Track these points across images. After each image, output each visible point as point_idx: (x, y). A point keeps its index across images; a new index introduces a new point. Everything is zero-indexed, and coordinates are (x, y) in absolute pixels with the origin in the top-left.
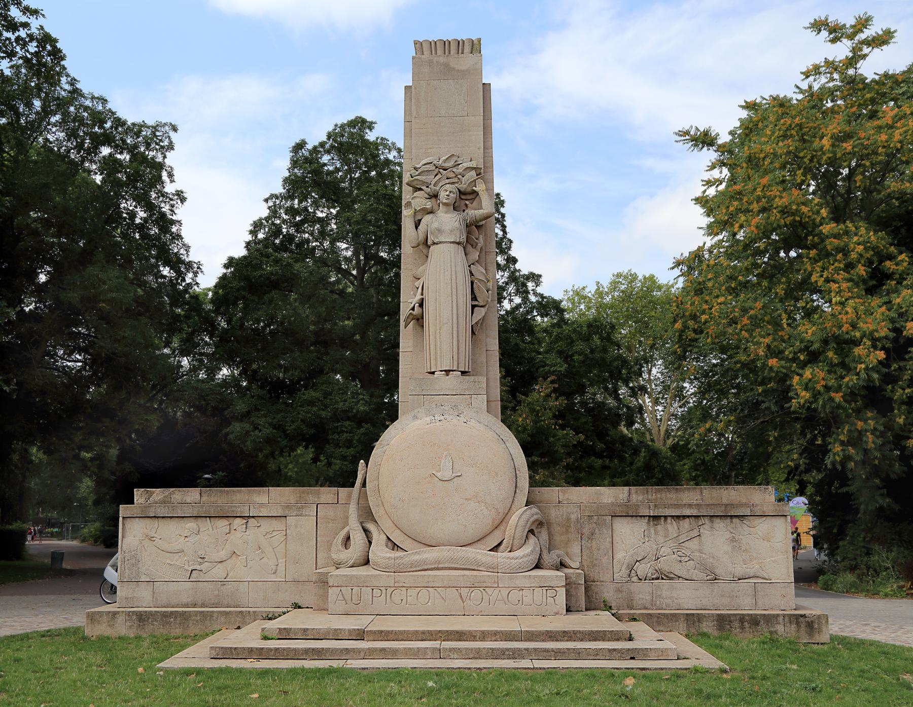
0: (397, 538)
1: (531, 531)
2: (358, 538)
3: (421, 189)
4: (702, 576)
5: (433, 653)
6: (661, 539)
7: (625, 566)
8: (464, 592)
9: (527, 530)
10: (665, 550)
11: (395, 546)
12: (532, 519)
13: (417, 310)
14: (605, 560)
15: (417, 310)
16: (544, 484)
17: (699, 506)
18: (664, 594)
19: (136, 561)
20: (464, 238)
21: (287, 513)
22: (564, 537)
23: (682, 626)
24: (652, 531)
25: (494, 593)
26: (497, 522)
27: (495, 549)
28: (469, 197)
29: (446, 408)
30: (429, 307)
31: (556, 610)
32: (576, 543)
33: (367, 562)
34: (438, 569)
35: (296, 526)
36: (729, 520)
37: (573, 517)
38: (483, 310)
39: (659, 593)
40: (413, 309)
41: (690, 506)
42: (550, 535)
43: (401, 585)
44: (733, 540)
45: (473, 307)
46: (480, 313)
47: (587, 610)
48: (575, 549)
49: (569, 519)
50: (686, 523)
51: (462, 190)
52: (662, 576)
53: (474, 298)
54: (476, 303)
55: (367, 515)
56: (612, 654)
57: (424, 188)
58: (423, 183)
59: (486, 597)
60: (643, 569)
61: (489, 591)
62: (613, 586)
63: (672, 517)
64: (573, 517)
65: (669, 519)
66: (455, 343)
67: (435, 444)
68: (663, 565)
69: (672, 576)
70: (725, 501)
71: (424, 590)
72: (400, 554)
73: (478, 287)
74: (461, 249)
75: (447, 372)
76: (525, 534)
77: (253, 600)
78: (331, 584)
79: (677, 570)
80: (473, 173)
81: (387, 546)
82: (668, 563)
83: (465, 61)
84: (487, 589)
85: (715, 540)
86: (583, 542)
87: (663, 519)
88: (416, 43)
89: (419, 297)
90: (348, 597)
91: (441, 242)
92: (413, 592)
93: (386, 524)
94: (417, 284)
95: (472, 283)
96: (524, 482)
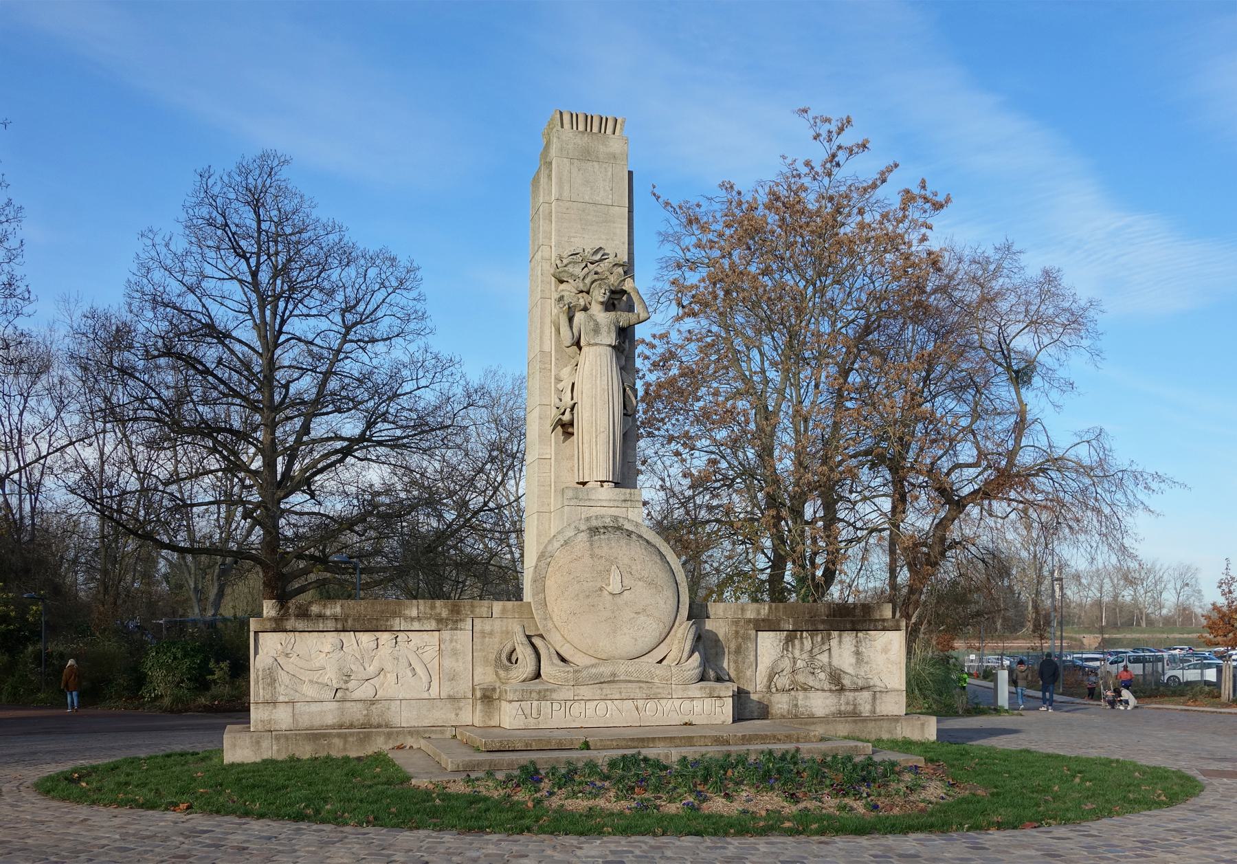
6: (797, 653)
8: (640, 703)
13: (567, 417)
14: (749, 673)
25: (667, 705)
35: (451, 641)
40: (563, 414)
44: (858, 653)
61: (663, 702)
68: (801, 678)
71: (602, 703)
90: (527, 711)
92: (591, 705)
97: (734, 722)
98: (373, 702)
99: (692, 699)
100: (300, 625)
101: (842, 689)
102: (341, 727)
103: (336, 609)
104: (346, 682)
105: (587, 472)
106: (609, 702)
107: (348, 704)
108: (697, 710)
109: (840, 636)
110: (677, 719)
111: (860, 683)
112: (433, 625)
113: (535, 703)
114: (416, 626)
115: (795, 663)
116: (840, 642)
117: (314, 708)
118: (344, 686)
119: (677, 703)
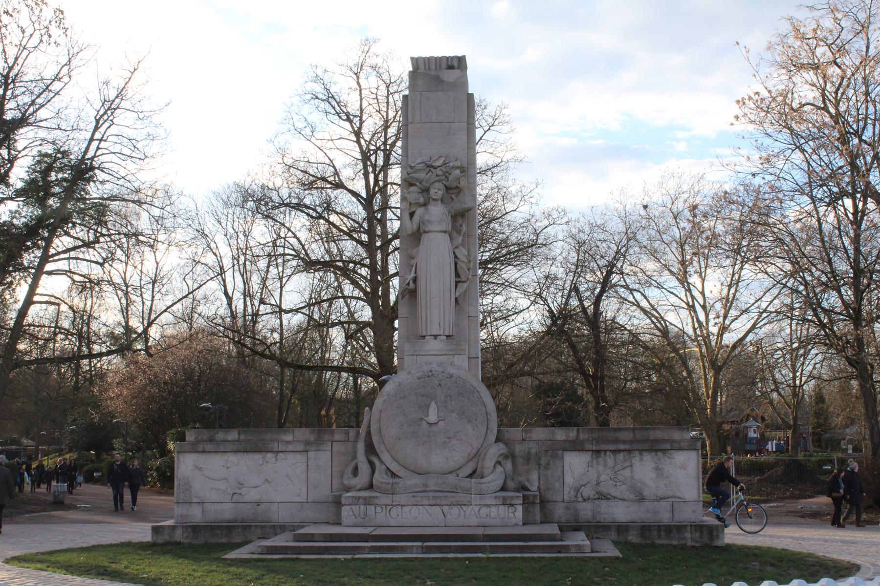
0: (394, 467)
1: (499, 463)
2: (364, 467)
3: (415, 185)
4: (632, 496)
6: (601, 468)
8: (446, 508)
9: (494, 462)
11: (394, 475)
12: (499, 453)
13: (412, 286)
14: (557, 485)
15: (412, 286)
16: (506, 426)
17: (631, 442)
18: (603, 510)
19: (188, 487)
20: (450, 228)
21: (308, 448)
22: (525, 467)
23: (614, 535)
24: (595, 462)
25: (468, 510)
27: (471, 476)
28: (454, 191)
30: (421, 284)
33: (371, 487)
35: (315, 459)
36: (654, 454)
37: (533, 451)
38: (465, 285)
40: (408, 284)
41: (624, 442)
42: (514, 465)
44: (657, 469)
45: (457, 283)
46: (463, 287)
47: (541, 523)
48: (534, 476)
49: (529, 453)
50: (621, 456)
52: (602, 496)
53: (457, 275)
56: (544, 549)
57: (418, 184)
58: (417, 180)
59: (462, 513)
60: (587, 492)
62: (564, 504)
64: (533, 451)
65: (608, 453)
68: (603, 489)
70: (652, 438)
71: (415, 508)
72: (397, 480)
73: (462, 267)
74: (447, 236)
75: (436, 337)
77: (282, 515)
78: (343, 503)
79: (614, 492)
80: (458, 172)
81: (387, 474)
83: (450, 76)
85: (644, 469)
89: (412, 275)
91: (430, 231)
93: (386, 457)
94: (412, 262)
95: (456, 264)
96: (494, 426)
97: (524, 524)
98: (258, 504)
99: (488, 506)
100: (208, 447)
101: (641, 499)
102: (235, 521)
103: (233, 435)
104: (240, 489)
105: (424, 329)
107: (241, 505)
108: (492, 515)
109: (641, 455)
110: (474, 521)
111: (661, 493)
113: (362, 507)
114: (290, 448)
116: (641, 459)
117: (218, 507)
118: (238, 491)
119: (476, 508)
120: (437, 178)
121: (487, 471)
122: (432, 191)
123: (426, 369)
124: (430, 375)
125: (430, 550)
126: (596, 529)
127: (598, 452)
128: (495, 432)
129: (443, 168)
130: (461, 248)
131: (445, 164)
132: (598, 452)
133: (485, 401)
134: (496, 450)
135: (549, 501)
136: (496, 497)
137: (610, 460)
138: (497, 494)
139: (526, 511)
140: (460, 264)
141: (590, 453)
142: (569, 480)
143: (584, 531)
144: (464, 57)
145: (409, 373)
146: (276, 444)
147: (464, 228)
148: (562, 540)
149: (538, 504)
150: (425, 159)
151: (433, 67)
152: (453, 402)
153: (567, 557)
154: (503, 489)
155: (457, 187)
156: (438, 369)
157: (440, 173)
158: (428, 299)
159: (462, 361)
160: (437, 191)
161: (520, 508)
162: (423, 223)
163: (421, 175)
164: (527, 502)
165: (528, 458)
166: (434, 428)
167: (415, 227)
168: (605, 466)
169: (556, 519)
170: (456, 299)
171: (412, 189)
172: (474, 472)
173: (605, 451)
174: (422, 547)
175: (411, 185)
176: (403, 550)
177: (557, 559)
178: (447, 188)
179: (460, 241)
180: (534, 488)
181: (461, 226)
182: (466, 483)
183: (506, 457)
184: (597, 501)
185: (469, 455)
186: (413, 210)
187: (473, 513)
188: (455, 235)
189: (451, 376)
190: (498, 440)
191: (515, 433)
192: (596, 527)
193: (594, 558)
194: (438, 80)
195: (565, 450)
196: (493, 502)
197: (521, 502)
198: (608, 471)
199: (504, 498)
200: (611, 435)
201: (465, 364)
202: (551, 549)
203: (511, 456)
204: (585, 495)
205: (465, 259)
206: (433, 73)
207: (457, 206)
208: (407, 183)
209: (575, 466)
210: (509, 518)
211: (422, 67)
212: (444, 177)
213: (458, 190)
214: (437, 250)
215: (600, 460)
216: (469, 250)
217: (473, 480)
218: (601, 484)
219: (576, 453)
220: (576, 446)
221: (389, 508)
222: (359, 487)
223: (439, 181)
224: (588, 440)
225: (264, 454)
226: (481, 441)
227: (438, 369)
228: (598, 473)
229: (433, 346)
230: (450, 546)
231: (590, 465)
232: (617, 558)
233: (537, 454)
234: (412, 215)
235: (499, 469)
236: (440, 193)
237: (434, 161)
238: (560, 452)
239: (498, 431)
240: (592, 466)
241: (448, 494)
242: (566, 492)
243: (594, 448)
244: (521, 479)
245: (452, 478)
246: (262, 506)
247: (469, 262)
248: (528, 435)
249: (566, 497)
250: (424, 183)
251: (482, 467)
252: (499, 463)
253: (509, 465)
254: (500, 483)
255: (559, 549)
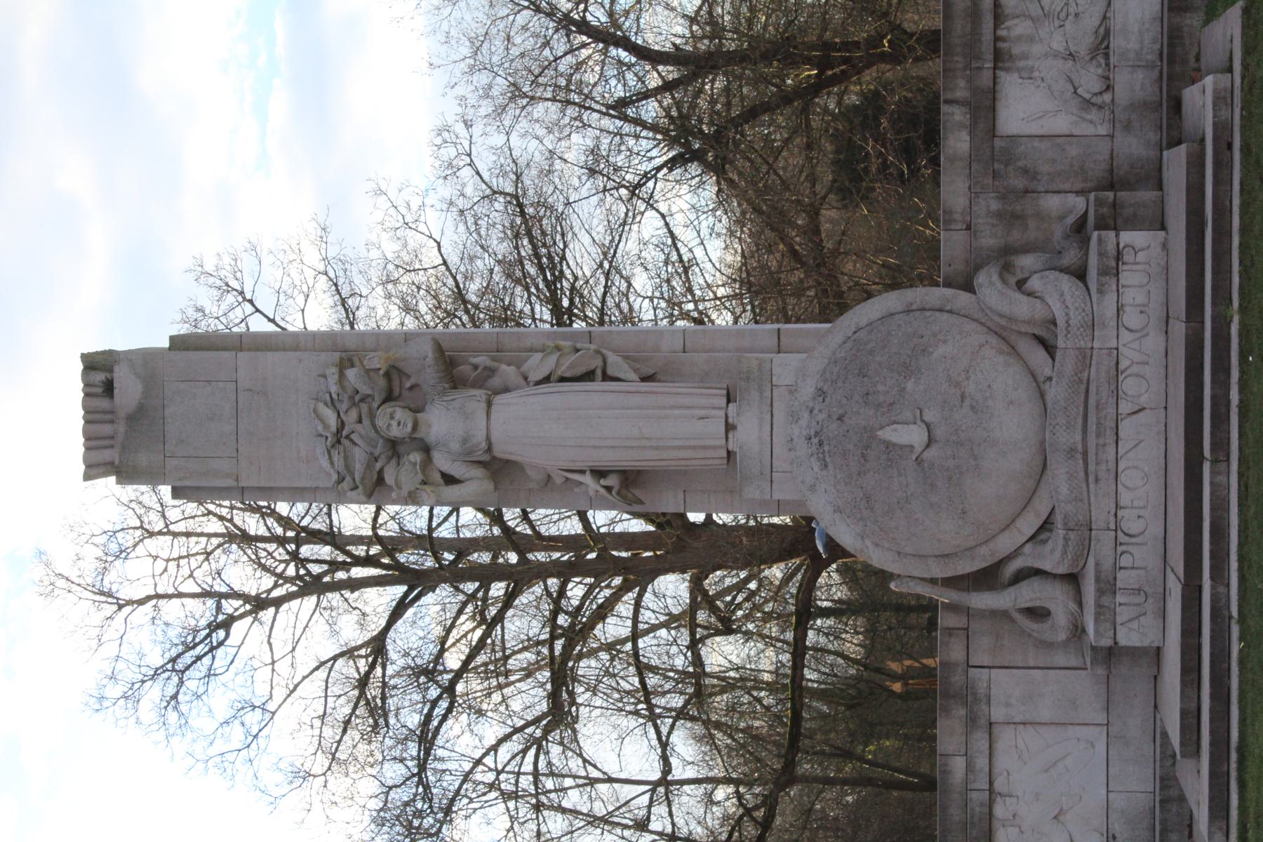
0: (1029, 524)
1: (1020, 284)
2: (1028, 594)
3: (381, 472)
5: (1219, 473)
6: (1036, 49)
7: (1084, 115)
8: (1125, 408)
10: (1057, 44)
11: (1046, 525)
12: (999, 285)
14: (1073, 151)
15: (612, 481)
18: (1133, 45)
20: (480, 393)
21: (983, 722)
22: (1032, 224)
23: (1193, 20)
24: (1022, 64)
26: (1005, 348)
27: (1050, 349)
28: (396, 383)
29: (797, 431)
30: (606, 459)
31: (1159, 249)
32: (1042, 202)
33: (1073, 579)
34: (1085, 454)
37: (995, 205)
38: (612, 358)
39: (1132, 55)
42: (1026, 249)
43: (1112, 519)
45: (606, 377)
46: (616, 364)
47: (1161, 189)
48: (1052, 203)
49: (999, 215)
51: (383, 396)
52: (1102, 47)
53: (588, 376)
54: (599, 372)
55: (987, 578)
56: (1222, 180)
57: (378, 466)
58: (369, 466)
59: (1135, 369)
60: (1090, 81)
61: (1124, 364)
63: (996, 27)
64: (995, 205)
66: (677, 412)
67: (863, 456)
68: (1083, 47)
69: (1102, 30)
71: (1122, 477)
72: (1058, 518)
73: (571, 367)
74: (498, 400)
75: (729, 427)
76: (1025, 299)
77: (1137, 784)
78: (1109, 642)
79: (1091, 20)
81: (1044, 542)
82: (1082, 34)
83: (129, 390)
84: (1121, 367)
86: (1041, 188)
87: (1001, 45)
88: (87, 477)
89: (587, 479)
91: (488, 438)
92: (1125, 498)
93: (1005, 544)
94: (559, 481)
95: (563, 379)
96: (936, 295)
97: (1163, 228)
105: (709, 454)
106: (1122, 466)
108: (1140, 299)
110: (1154, 342)
112: (980, 742)
113: (1120, 598)
115: (1056, 55)
119: (1126, 336)
120: (366, 421)
121: (1039, 311)
122: (395, 432)
123: (803, 449)
124: (817, 439)
125: (1220, 445)
126: (1177, 62)
127: (998, 56)
128: (949, 292)
129: (343, 407)
130: (525, 368)
131: (333, 404)
132: (998, 56)
133: (878, 315)
134: (992, 291)
135: (1111, 171)
136: (1100, 292)
137: (1017, 28)
138: (1093, 287)
139: (1133, 223)
140: (563, 370)
141: (1000, 73)
142: (1061, 124)
143: (1180, 89)
144: (85, 357)
145: (812, 488)
146: (974, 795)
147: (481, 360)
148: (1203, 140)
149: (1118, 195)
150: (320, 449)
151: (107, 429)
152: (880, 388)
153: (1242, 127)
154: (1080, 275)
155: (387, 375)
156: (803, 423)
157: (353, 414)
158: (648, 443)
159: (785, 368)
160: (396, 422)
161: (1126, 237)
162: (470, 453)
163: (359, 456)
164: (1113, 220)
165: (1011, 218)
166: (939, 432)
167: (478, 472)
168: (1031, 39)
169: (1153, 153)
170: (645, 379)
171: (389, 478)
172: (1042, 341)
173: (997, 39)
174: (1215, 462)
175: (380, 480)
176: (1220, 506)
177: (1246, 149)
178: (389, 398)
179: (511, 370)
180: (1079, 203)
181: (476, 367)
182: (1067, 361)
183: (1007, 268)
184: (1113, 60)
185: (1001, 352)
186: (438, 478)
187: (1136, 345)
188: (496, 382)
189: (821, 393)
190: (969, 287)
191: (953, 245)
192: (1171, 61)
193: (1245, 66)
194: (138, 417)
195: (992, 132)
196: (1111, 299)
197: (1112, 234)
198: (1043, 33)
199: (1103, 272)
200: (960, 26)
201: (793, 359)
202: (1222, 166)
203: (1005, 257)
204: (1097, 86)
205: (553, 359)
206: (122, 428)
207: (429, 376)
208: (375, 489)
209: (1031, 108)
210: (1148, 262)
211: (107, 455)
212: (364, 407)
213: (393, 373)
214: (528, 422)
215: (1016, 50)
216: (532, 350)
217: (1061, 343)
218: (1073, 48)
219: (999, 105)
220: (985, 107)
221: (1122, 538)
222: (1073, 606)
223: (372, 416)
224: (970, 80)
225: (996, 824)
226: (972, 326)
227: (803, 423)
228: (1046, 55)
229: (749, 434)
230: (1213, 397)
231: (1028, 75)
232: (1246, 11)
233: (1002, 198)
234: (449, 480)
235: (1035, 283)
236: (400, 414)
237: (326, 427)
238: (998, 143)
239: (948, 285)
240: (1032, 70)
241: (1092, 401)
242: (1091, 130)
243: (989, 65)
244: (1058, 232)
245: (1055, 392)
246: (1117, 828)
247: (558, 348)
248: (957, 217)
249: (1102, 130)
250: (377, 453)
251: (1030, 322)
252: (1020, 284)
253: (1026, 262)
254: (1067, 284)
255: (1222, 146)
